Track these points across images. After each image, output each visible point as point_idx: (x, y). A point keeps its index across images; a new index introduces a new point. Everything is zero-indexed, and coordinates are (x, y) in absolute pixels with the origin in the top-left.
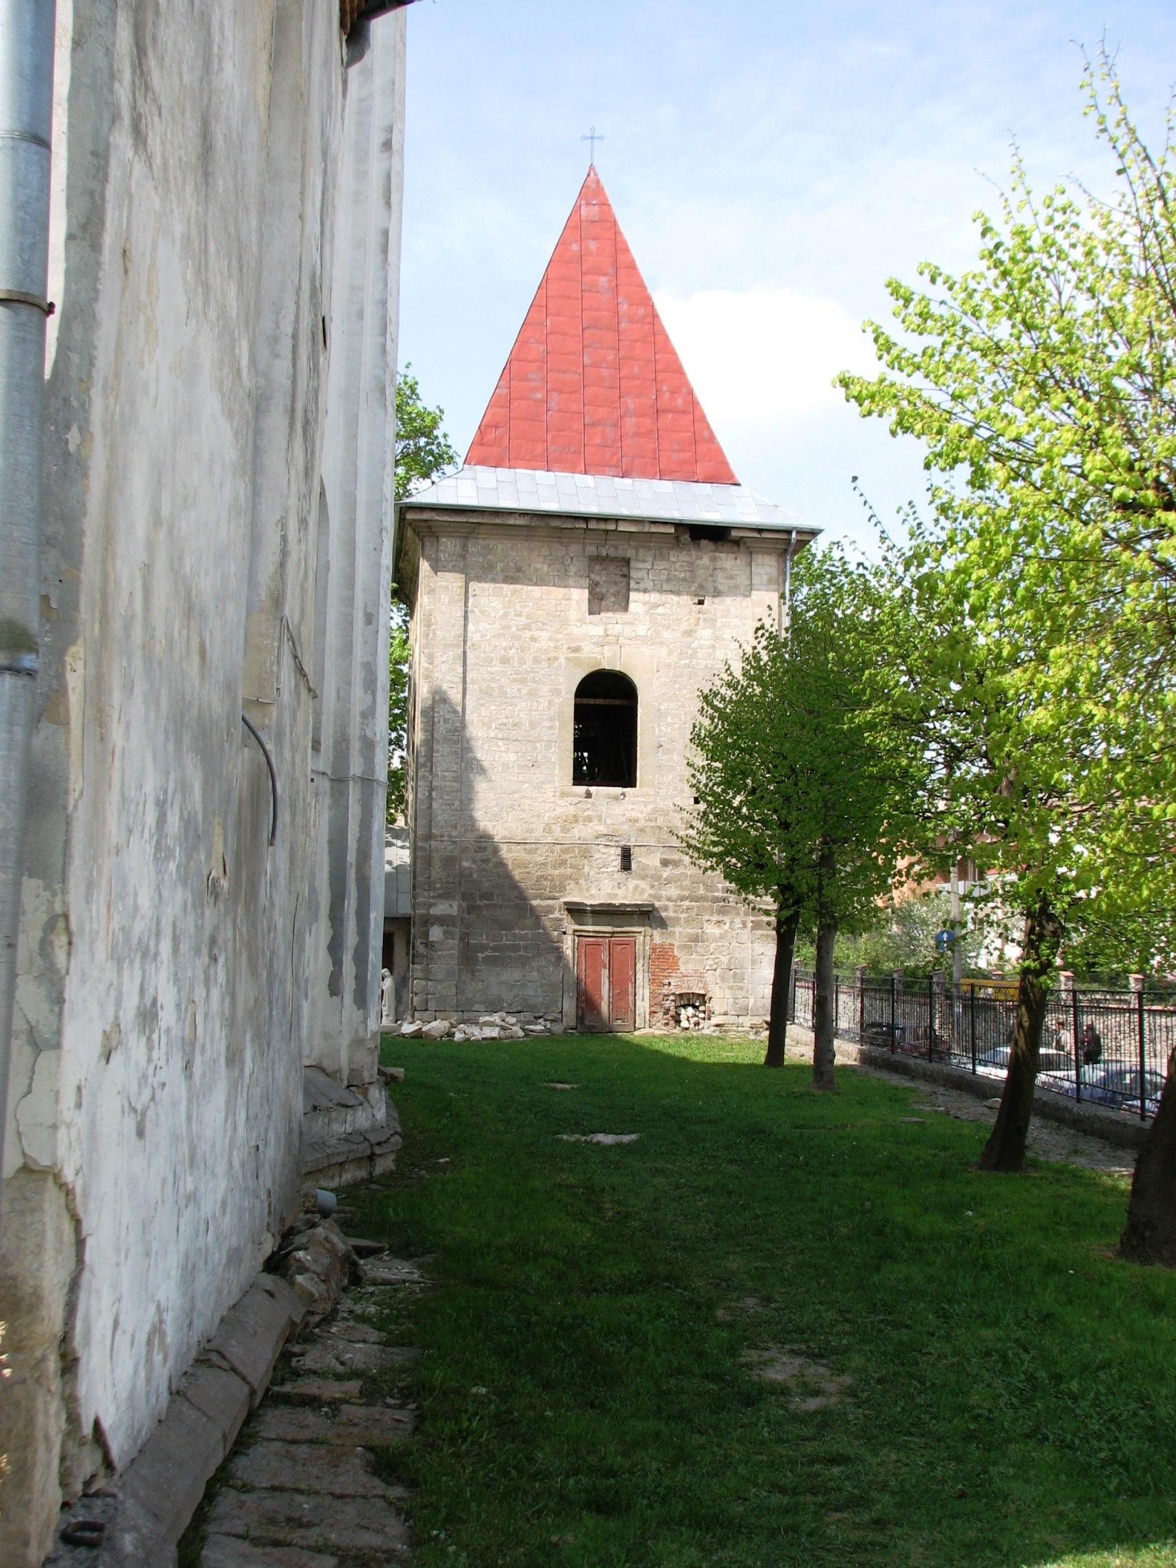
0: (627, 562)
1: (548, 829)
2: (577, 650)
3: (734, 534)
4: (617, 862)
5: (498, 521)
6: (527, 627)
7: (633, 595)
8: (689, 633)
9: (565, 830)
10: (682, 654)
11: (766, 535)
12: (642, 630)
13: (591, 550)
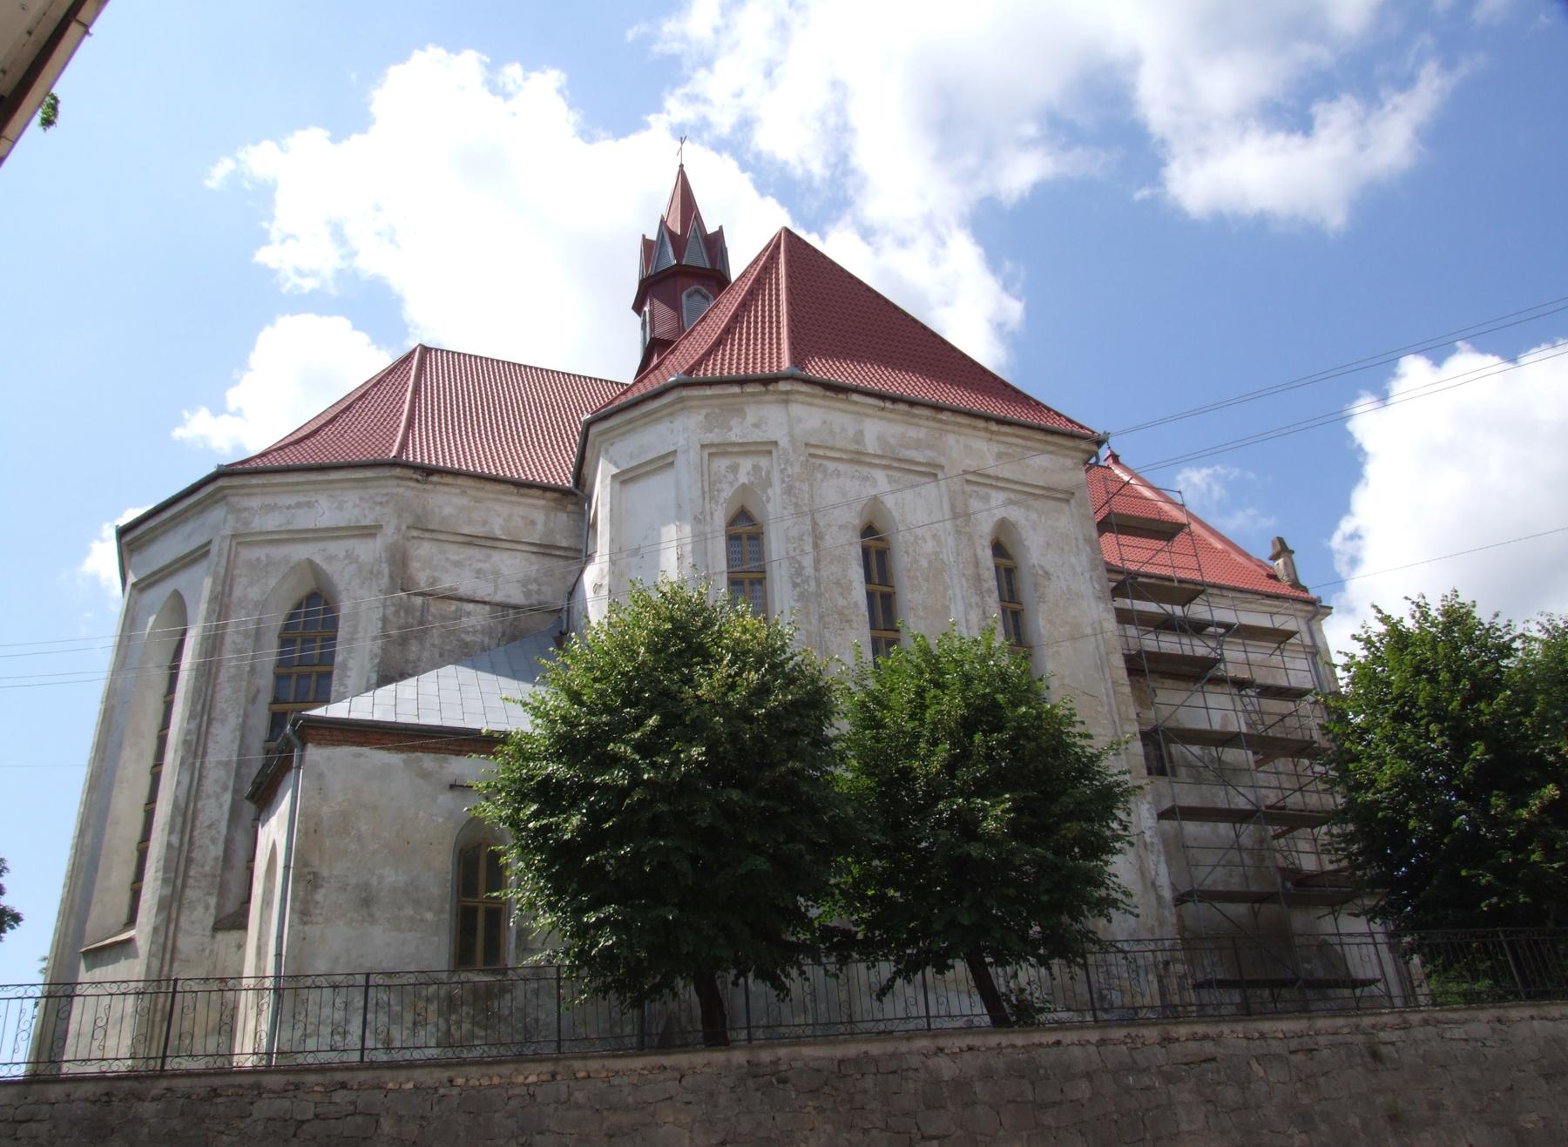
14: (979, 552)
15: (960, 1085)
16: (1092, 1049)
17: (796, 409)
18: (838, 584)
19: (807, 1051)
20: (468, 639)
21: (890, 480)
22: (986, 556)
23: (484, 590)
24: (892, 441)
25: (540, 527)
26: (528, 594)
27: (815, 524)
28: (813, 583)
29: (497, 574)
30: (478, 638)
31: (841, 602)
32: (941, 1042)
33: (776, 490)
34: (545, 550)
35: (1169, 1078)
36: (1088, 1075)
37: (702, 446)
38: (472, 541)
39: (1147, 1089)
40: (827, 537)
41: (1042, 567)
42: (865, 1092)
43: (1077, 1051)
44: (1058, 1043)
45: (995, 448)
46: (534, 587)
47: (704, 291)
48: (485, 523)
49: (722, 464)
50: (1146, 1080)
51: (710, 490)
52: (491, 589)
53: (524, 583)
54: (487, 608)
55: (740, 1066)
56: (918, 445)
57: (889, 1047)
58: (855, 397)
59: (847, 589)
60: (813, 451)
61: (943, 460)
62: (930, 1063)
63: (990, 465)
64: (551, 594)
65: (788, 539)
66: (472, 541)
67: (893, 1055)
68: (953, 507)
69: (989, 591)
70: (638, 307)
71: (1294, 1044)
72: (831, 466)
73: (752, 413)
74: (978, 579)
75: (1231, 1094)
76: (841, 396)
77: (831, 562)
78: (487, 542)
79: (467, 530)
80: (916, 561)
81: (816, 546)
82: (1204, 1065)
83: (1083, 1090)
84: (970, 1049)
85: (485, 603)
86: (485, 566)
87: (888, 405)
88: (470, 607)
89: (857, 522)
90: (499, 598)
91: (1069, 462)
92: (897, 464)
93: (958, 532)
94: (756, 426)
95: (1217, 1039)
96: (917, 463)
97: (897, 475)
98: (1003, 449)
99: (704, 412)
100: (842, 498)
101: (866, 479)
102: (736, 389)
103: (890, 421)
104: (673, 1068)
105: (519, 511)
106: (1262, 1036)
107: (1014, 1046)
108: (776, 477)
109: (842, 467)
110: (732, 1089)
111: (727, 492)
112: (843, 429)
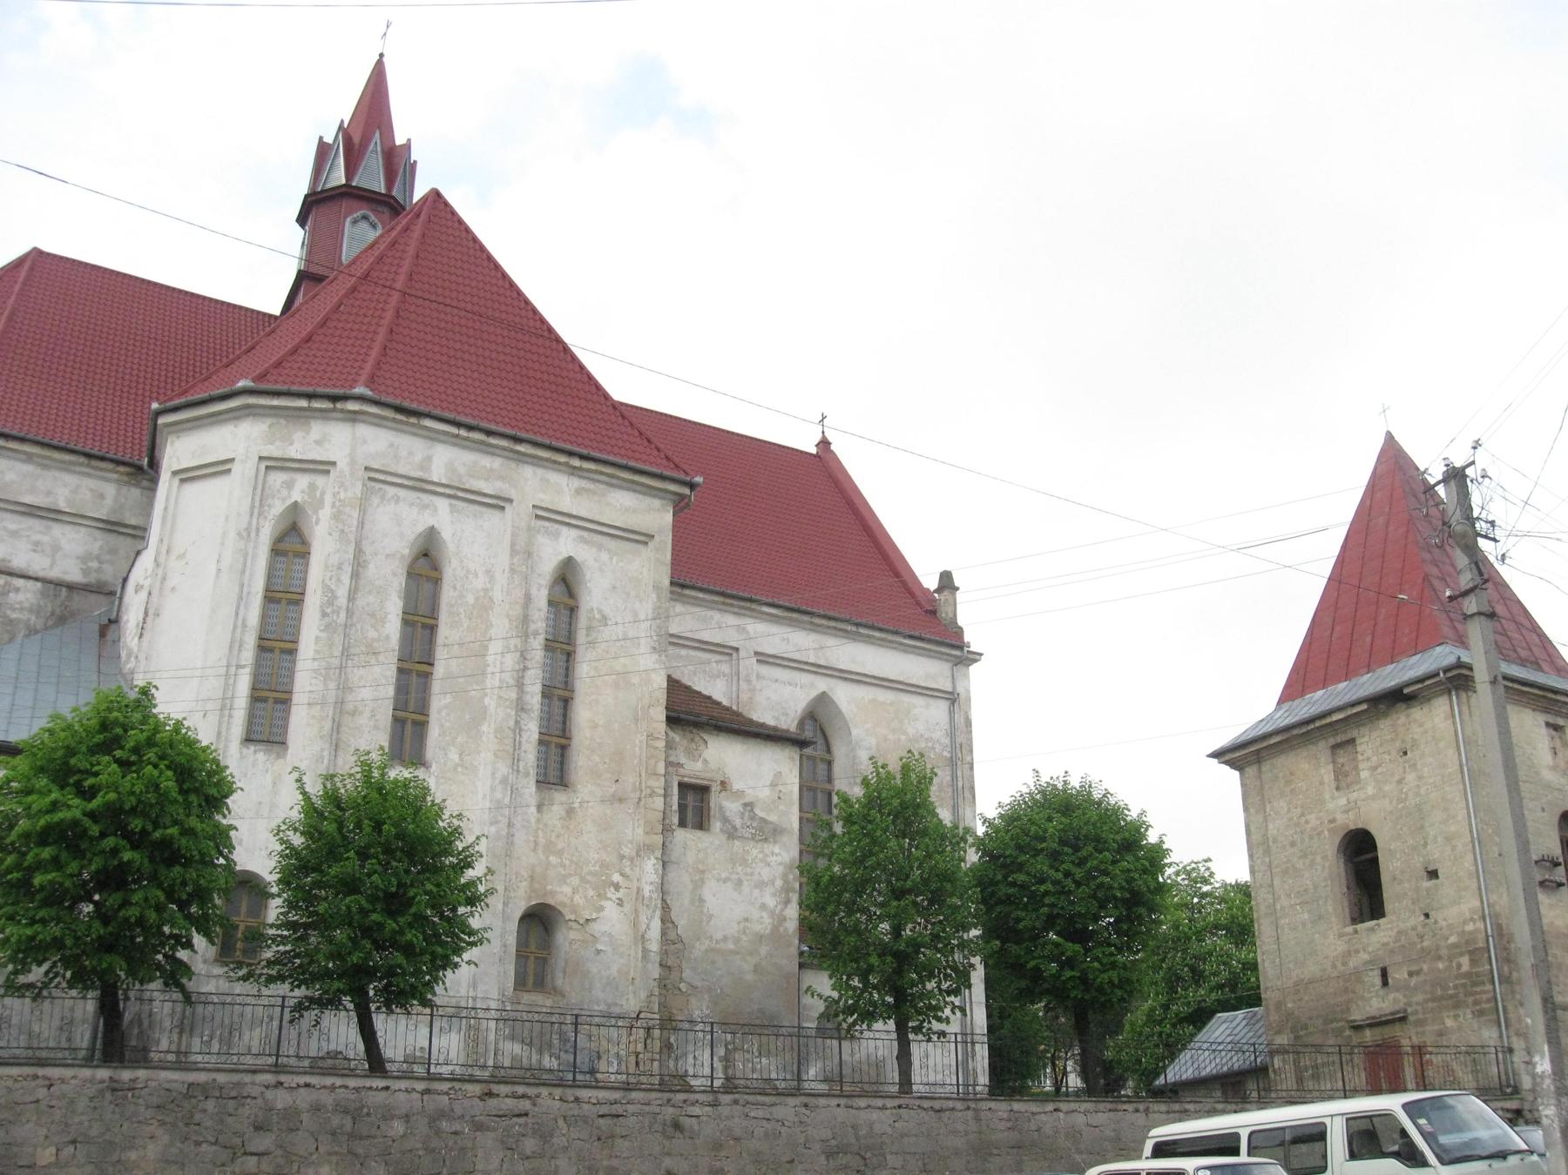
0: (1352, 741)
1: (1334, 966)
2: (1332, 821)
3: (1406, 691)
4: (1378, 981)
5: (1265, 744)
6: (1303, 815)
7: (1361, 766)
8: (1400, 782)
9: (1344, 964)
10: (1400, 801)
11: (1428, 682)
12: (1370, 790)
13: (1332, 741)
14: (534, 591)
15: (290, 1114)
16: (415, 1096)
17: (364, 430)
18: (372, 615)
19: (163, 1074)
20: (14, 616)
21: (453, 509)
22: (541, 596)
23: (39, 564)
24: (462, 470)
25: (109, 501)
26: (86, 572)
27: (359, 551)
28: (343, 615)
29: (56, 548)
30: (24, 616)
31: (372, 634)
32: (283, 1078)
33: (325, 514)
34: (112, 526)
35: (479, 1127)
36: (407, 1118)
37: (261, 458)
38: (32, 511)
39: (456, 1133)
40: (371, 566)
41: (600, 611)
42: (205, 1111)
43: (402, 1096)
44: (387, 1088)
45: (576, 483)
46: (94, 564)
47: (373, 218)
48: (49, 493)
49: (277, 478)
50: (457, 1126)
51: (259, 503)
52: (46, 562)
53: (84, 559)
54: (39, 585)
55: (102, 1082)
56: (489, 475)
57: (236, 1077)
58: (428, 423)
59: (379, 620)
60: (373, 475)
61: (513, 494)
63: (567, 503)
64: (109, 574)
65: (326, 566)
66: (32, 511)
68: (513, 544)
69: (536, 634)
70: (302, 220)
71: (604, 1110)
72: (391, 491)
73: (317, 429)
74: (526, 619)
75: (530, 1145)
76: (413, 420)
77: (370, 592)
78: (51, 514)
79: (28, 499)
80: (462, 596)
81: (355, 576)
82: (515, 1120)
84: (307, 1085)
85: (37, 579)
86: (45, 539)
87: (463, 433)
88: (20, 582)
89: (406, 551)
90: (55, 574)
91: (657, 503)
92: (461, 495)
93: (513, 571)
94: (318, 442)
95: (533, 1100)
96: (485, 495)
97: (460, 504)
98: (584, 484)
99: (269, 421)
100: (397, 524)
101: (426, 507)
102: (303, 403)
103: (464, 447)
104: (45, 1078)
105: (91, 483)
106: (577, 1099)
107: (346, 1087)
108: (328, 500)
109: (402, 493)
110: (91, 1099)
111: (277, 508)
112: (411, 453)
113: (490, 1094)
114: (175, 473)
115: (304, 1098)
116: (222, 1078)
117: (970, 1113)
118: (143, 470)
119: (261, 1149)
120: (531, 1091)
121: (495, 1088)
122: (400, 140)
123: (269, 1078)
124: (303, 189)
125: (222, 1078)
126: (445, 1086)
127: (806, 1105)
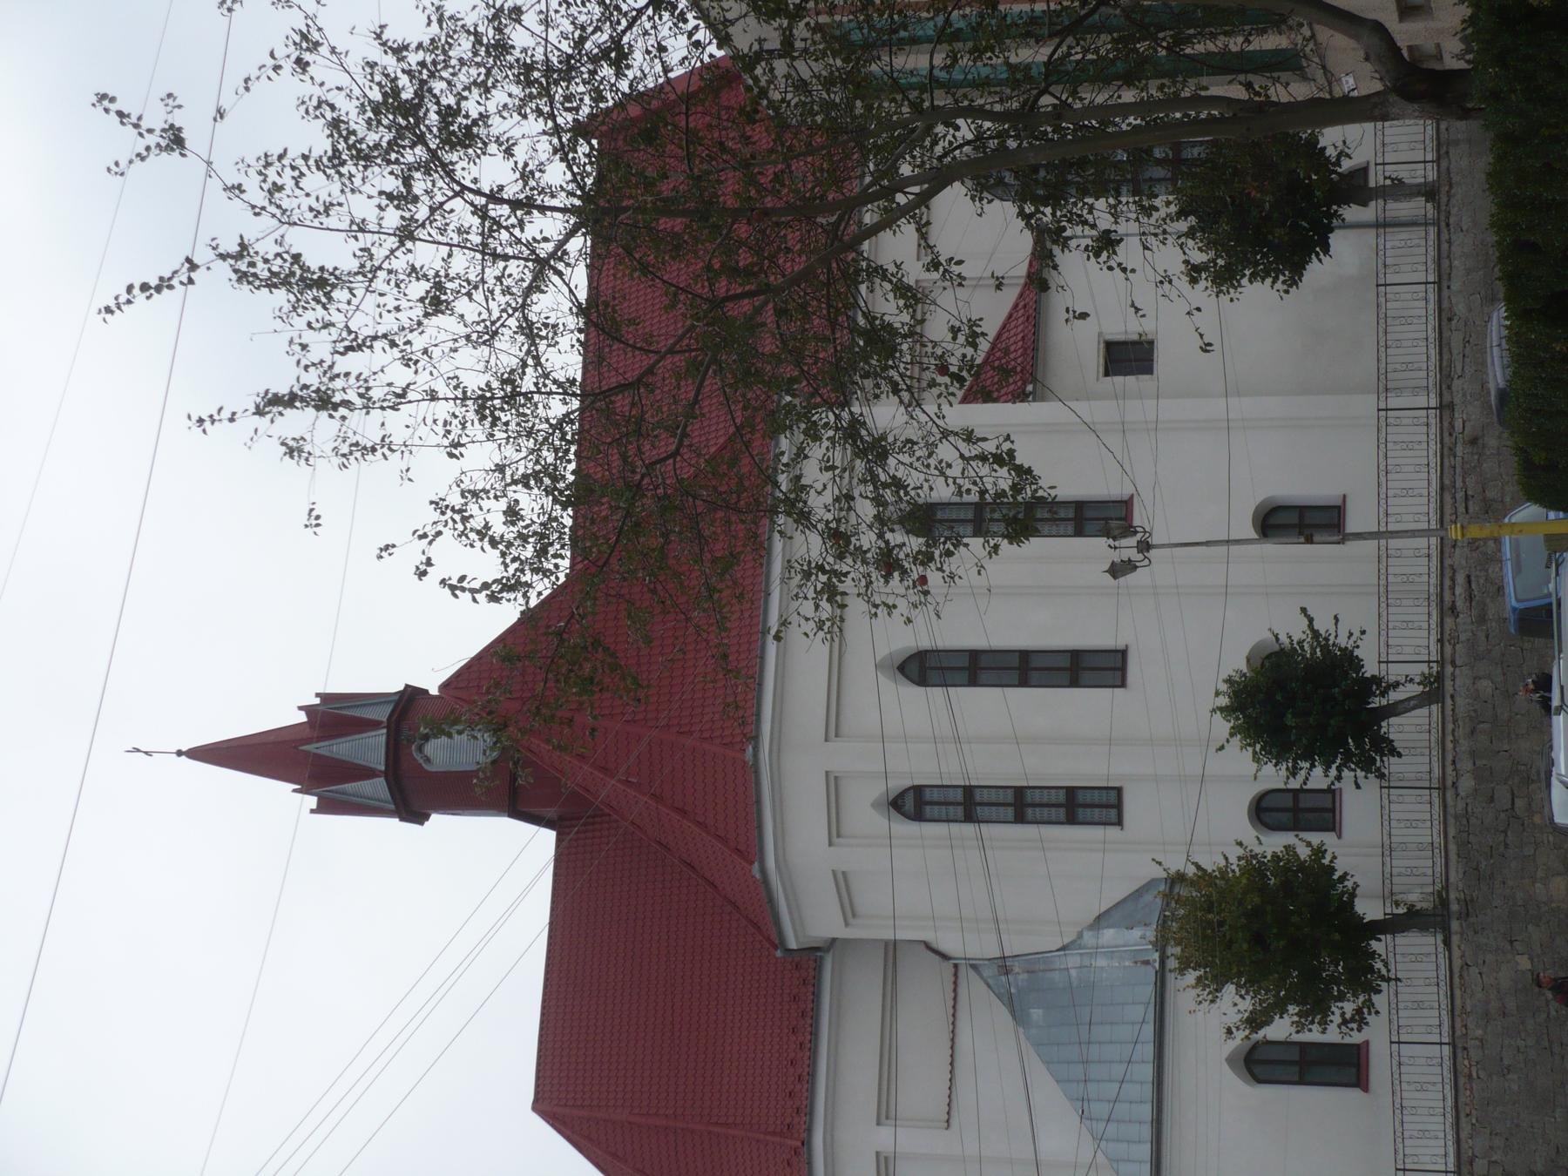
16: (1457, 671)
32: (1449, 783)
36: (1476, 678)
43: (1458, 682)
57: (1451, 821)
62: (1463, 794)
67: (1456, 817)
71: (1461, 509)
83: (1485, 686)
84: (1454, 762)
113: (1453, 608)
114: (847, 924)
115: (1466, 765)
116: (1452, 832)
117: (1452, 151)
118: (810, 960)
119: (1509, 796)
120: (1448, 573)
121: (1447, 603)
122: (302, 717)
123: (1450, 794)
124: (393, 823)
125: (1452, 832)
126: (1448, 649)
127: (1450, 320)
